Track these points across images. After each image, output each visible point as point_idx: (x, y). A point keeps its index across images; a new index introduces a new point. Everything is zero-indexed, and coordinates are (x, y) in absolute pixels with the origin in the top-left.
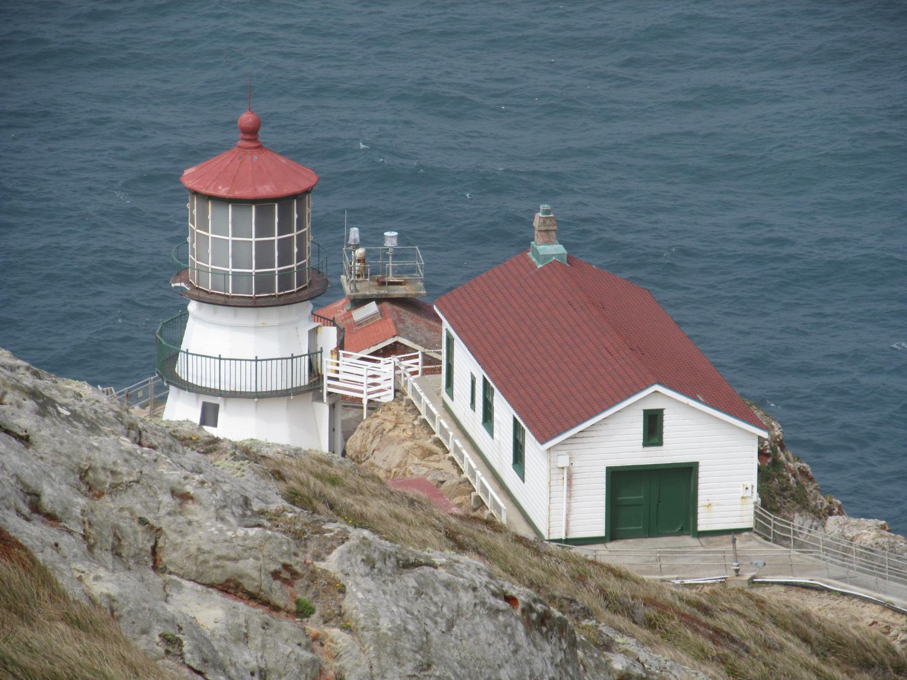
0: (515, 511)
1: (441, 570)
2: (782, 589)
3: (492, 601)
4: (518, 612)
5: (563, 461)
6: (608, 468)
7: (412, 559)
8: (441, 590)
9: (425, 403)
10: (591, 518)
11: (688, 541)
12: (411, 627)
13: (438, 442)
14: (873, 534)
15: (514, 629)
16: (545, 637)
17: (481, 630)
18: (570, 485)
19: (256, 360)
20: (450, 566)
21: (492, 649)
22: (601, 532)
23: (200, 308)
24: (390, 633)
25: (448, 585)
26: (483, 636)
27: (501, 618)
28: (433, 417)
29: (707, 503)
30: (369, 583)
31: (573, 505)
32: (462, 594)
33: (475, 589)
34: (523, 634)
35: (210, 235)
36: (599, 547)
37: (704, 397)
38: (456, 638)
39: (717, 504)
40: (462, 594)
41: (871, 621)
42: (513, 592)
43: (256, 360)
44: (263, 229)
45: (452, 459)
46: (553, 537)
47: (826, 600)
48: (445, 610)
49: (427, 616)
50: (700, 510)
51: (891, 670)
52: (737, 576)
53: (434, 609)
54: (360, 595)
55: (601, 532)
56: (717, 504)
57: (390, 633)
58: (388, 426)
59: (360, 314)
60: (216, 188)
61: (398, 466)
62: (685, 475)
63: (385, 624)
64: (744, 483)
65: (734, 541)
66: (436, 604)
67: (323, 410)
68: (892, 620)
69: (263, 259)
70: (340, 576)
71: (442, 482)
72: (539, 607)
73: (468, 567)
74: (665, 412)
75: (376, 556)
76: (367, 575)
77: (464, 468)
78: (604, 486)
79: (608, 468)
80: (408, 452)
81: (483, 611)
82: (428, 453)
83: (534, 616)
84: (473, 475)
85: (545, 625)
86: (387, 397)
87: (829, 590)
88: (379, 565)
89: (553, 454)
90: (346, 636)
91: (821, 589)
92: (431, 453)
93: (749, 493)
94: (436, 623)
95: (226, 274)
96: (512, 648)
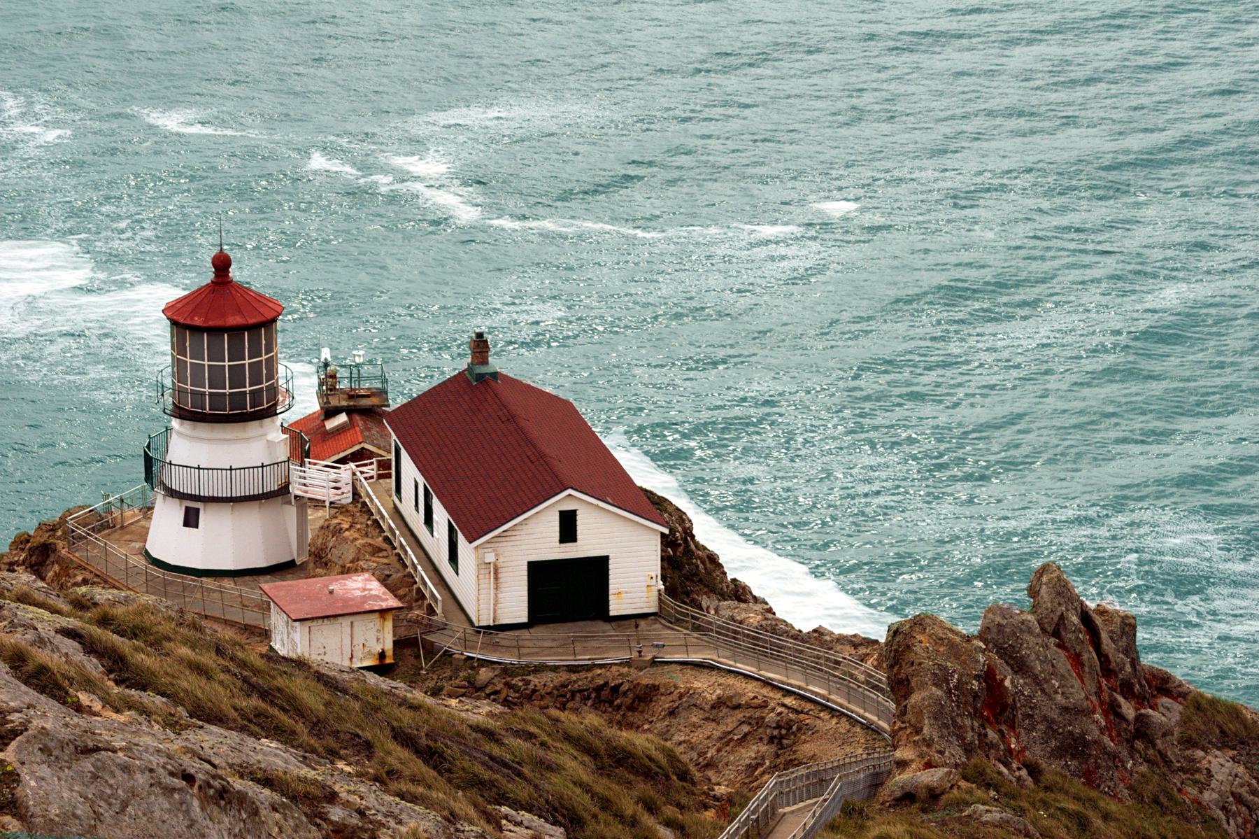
0: (450, 602)
1: (120, 754)
2: (679, 668)
3: (169, 780)
4: (195, 790)
5: (490, 558)
6: (529, 563)
7: (91, 744)
8: (118, 773)
9: (378, 504)
10: (515, 606)
11: (601, 626)
12: (79, 812)
13: (387, 539)
14: (759, 618)
15: (189, 805)
16: (224, 810)
17: (156, 808)
18: (496, 578)
19: (231, 469)
20: (127, 750)
21: (165, 827)
22: (524, 618)
23: (181, 424)
24: (57, 819)
25: (126, 769)
26: (157, 814)
27: (176, 796)
28: (383, 517)
30: (45, 771)
31: (500, 595)
32: (138, 776)
33: (151, 771)
34: (198, 810)
35: (189, 360)
36: (524, 633)
37: (613, 499)
38: (130, 817)
40: (138, 776)
41: (752, 695)
42: (192, 771)
43: (231, 469)
44: (236, 354)
45: (398, 555)
46: (482, 624)
47: (714, 678)
48: (120, 792)
49: (101, 798)
50: (611, 597)
51: (675, 778)
53: (109, 791)
54: (33, 783)
55: (524, 618)
57: (57, 819)
58: (345, 526)
59: (331, 424)
60: (192, 319)
61: (352, 562)
63: (54, 810)
65: (637, 626)
66: (111, 786)
67: (291, 512)
68: (771, 694)
69: (237, 380)
70: (16, 765)
71: (389, 576)
72: (216, 784)
73: (147, 750)
75: (51, 745)
76: (44, 762)
77: (408, 563)
78: (526, 578)
79: (529, 563)
80: (359, 549)
81: (158, 790)
82: (377, 551)
83: (211, 792)
84: (416, 569)
85: (223, 799)
86: (347, 499)
87: (719, 669)
88: (55, 753)
89: (480, 551)
90: (15, 822)
91: (712, 668)
92: (381, 550)
93: (654, 582)
94: (110, 804)
95: (203, 394)
96: (186, 823)
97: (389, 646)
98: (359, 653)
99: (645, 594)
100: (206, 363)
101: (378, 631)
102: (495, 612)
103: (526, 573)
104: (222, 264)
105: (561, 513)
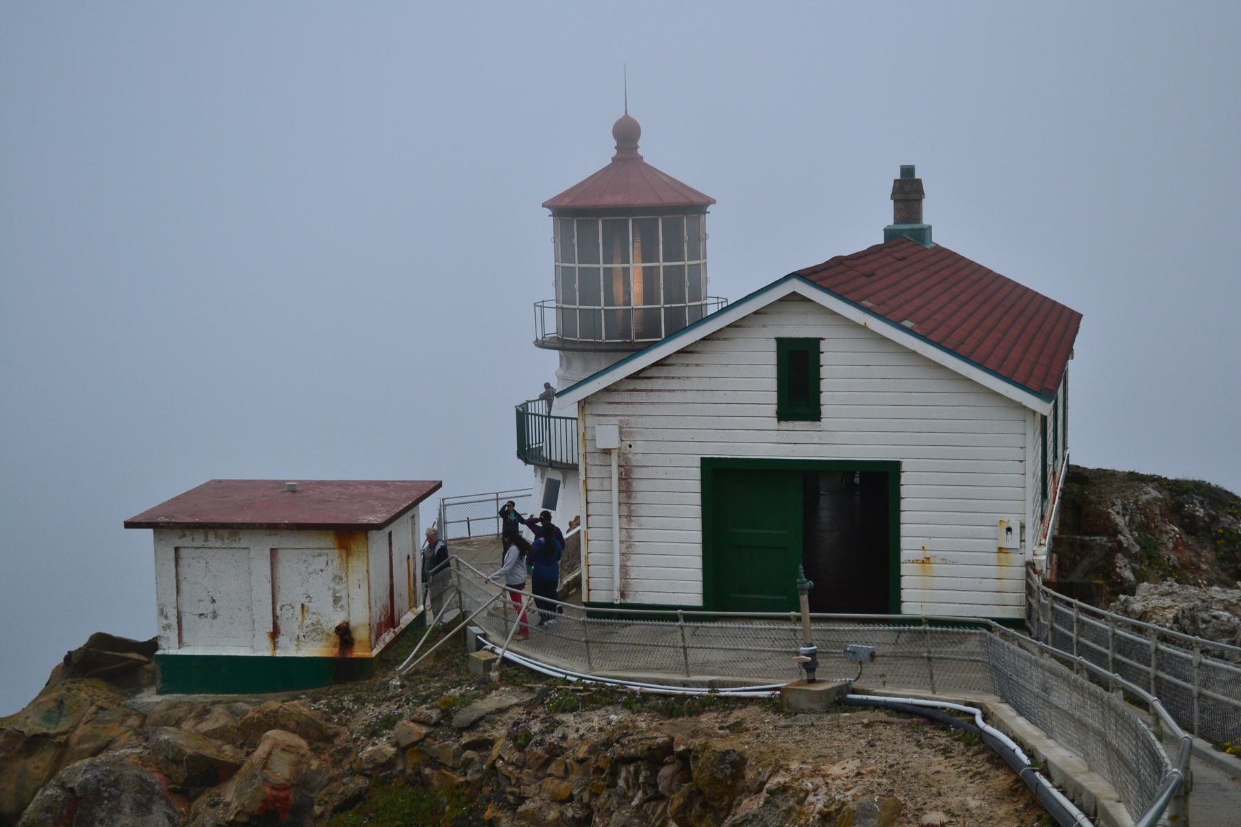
6: (704, 461)
10: (671, 566)
29: (920, 555)
31: (637, 535)
39: (944, 561)
50: (905, 569)
52: (812, 681)
55: (697, 601)
56: (944, 561)
62: (872, 490)
64: (1005, 517)
74: (823, 346)
78: (697, 499)
79: (704, 461)
97: (360, 616)
98: (290, 626)
99: (993, 571)
100: (576, 265)
101: (337, 579)
102: (624, 569)
103: (697, 486)
104: (627, 134)
105: (780, 341)
